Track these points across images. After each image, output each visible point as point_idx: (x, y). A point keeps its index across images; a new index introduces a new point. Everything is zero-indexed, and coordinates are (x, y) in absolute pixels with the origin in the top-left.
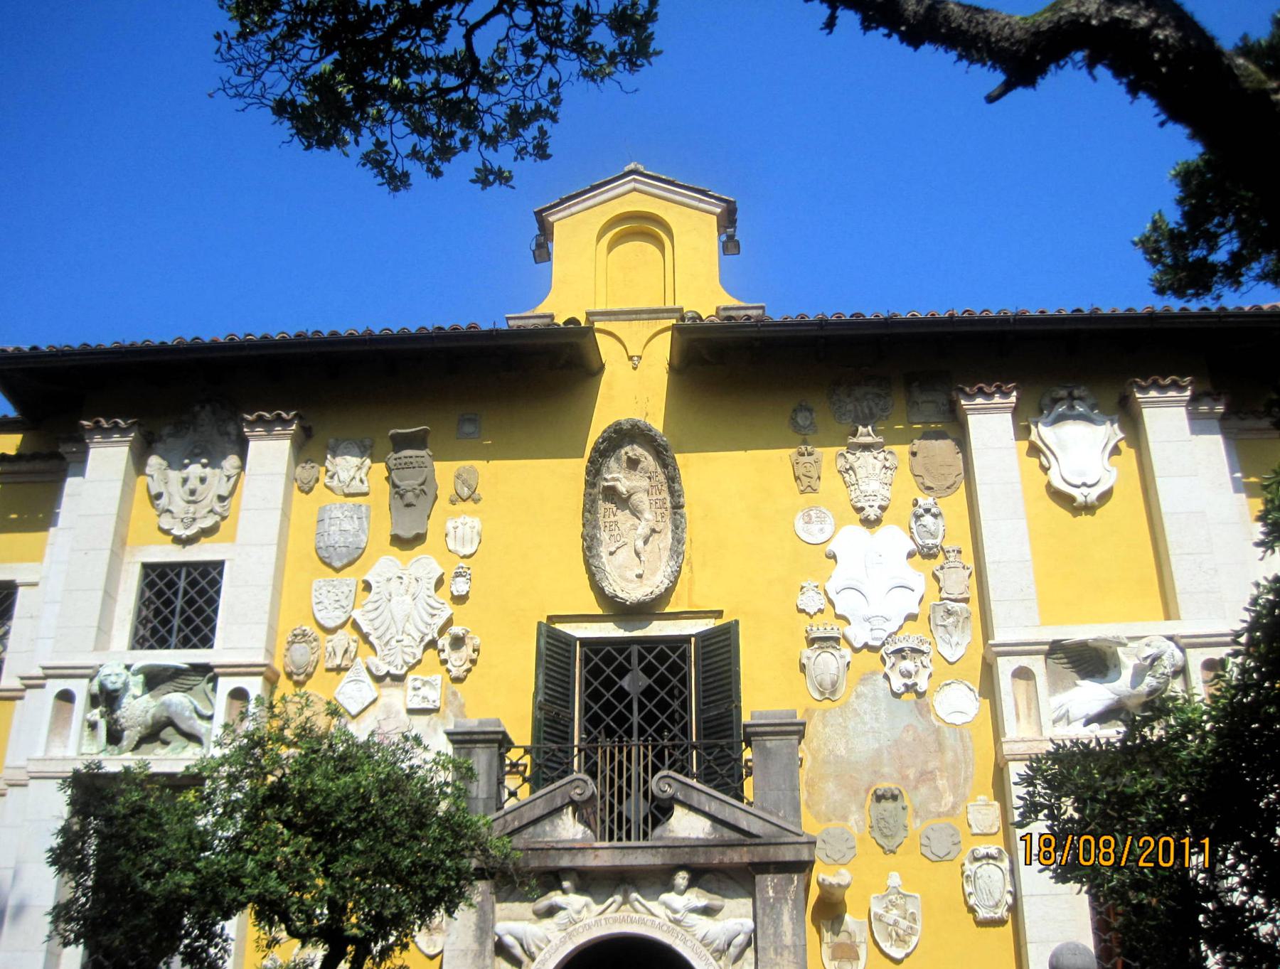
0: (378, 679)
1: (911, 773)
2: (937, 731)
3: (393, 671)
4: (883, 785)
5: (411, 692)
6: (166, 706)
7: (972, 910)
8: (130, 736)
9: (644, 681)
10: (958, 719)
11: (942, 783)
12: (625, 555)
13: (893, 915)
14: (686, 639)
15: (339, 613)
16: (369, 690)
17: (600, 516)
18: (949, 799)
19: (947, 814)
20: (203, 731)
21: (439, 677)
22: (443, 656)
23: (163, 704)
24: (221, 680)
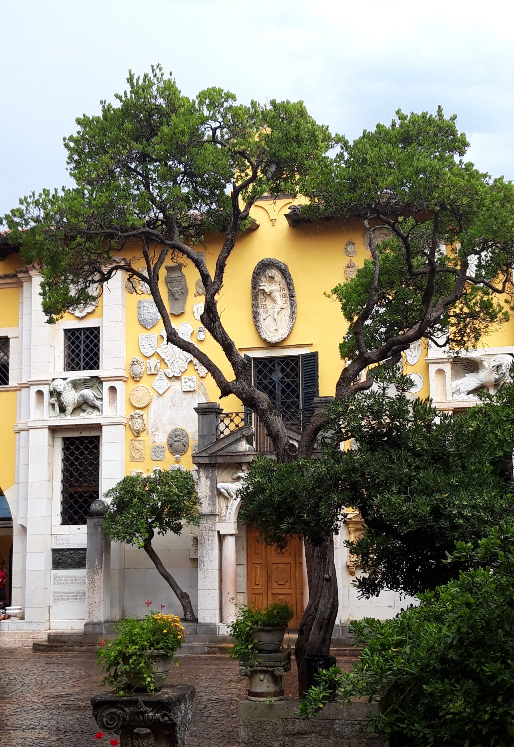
0: (170, 378)
3: (176, 375)
5: (184, 384)
6: (82, 396)
8: (69, 409)
9: (281, 375)
12: (270, 320)
14: (298, 357)
15: (151, 349)
16: (166, 383)
17: (259, 302)
20: (99, 405)
21: (195, 377)
22: (196, 367)
23: (81, 395)
24: (104, 383)
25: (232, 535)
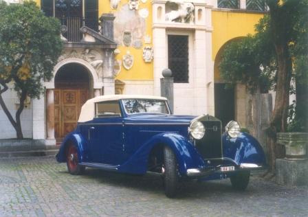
1: (133, 28)
2: (139, 19)
4: (127, 31)
7: (144, 60)
10: (144, 17)
11: (139, 31)
13: (127, 60)
18: (141, 35)
19: (140, 38)
25: (52, 89)
